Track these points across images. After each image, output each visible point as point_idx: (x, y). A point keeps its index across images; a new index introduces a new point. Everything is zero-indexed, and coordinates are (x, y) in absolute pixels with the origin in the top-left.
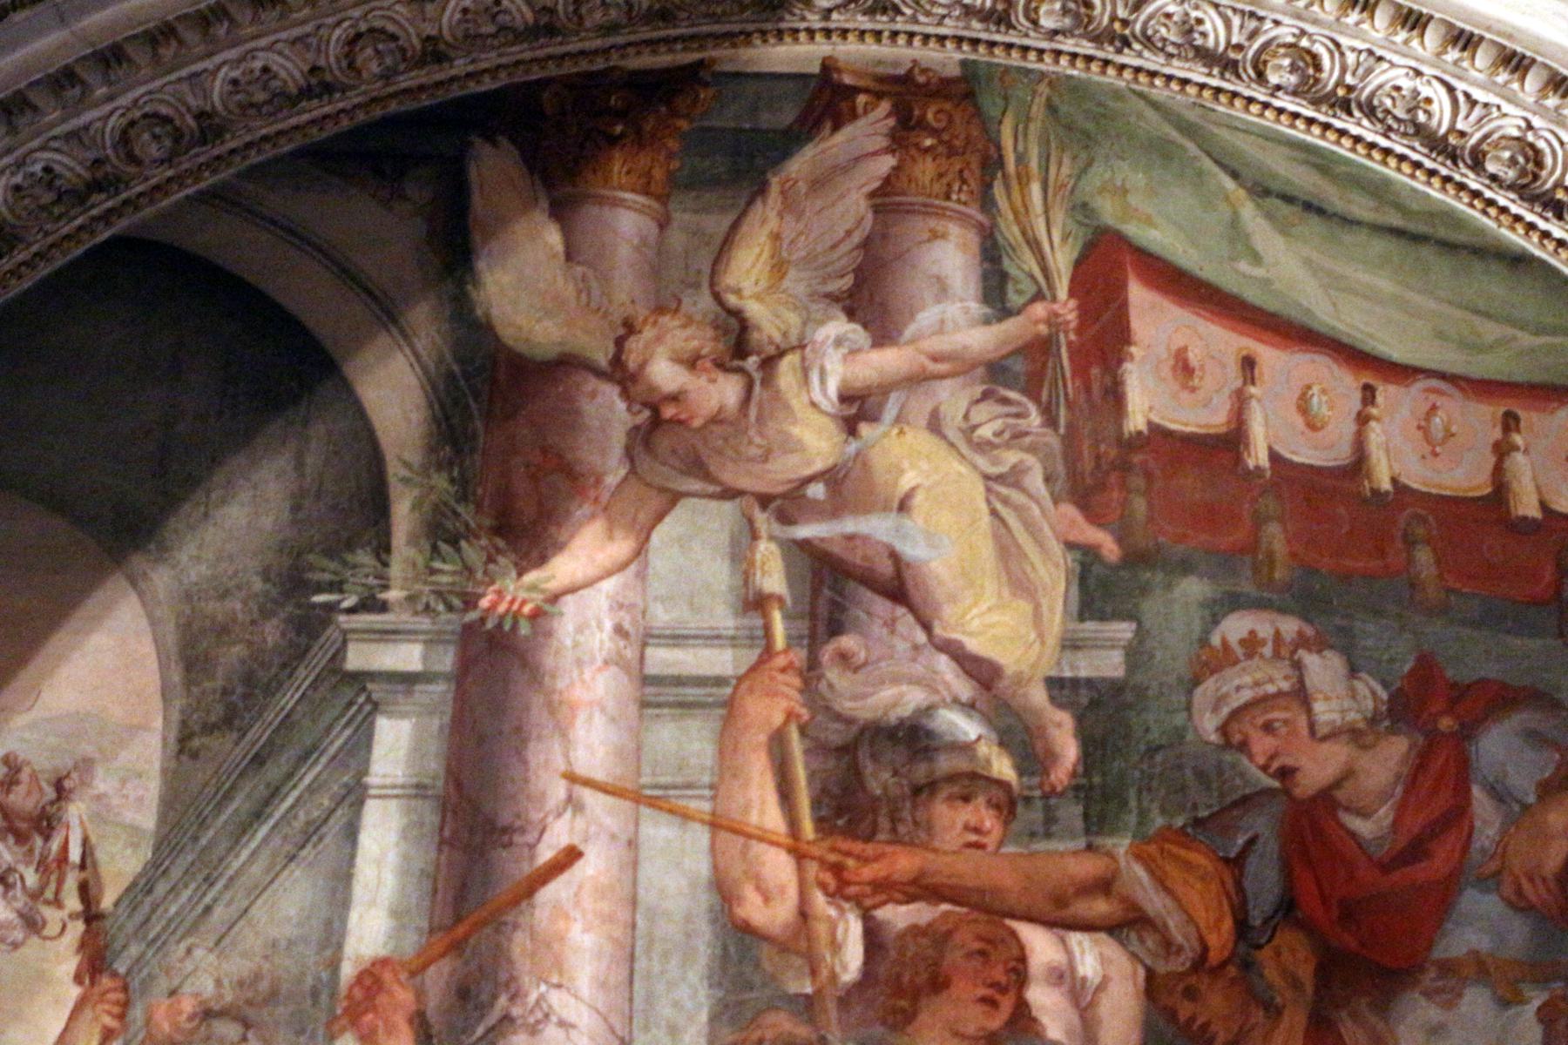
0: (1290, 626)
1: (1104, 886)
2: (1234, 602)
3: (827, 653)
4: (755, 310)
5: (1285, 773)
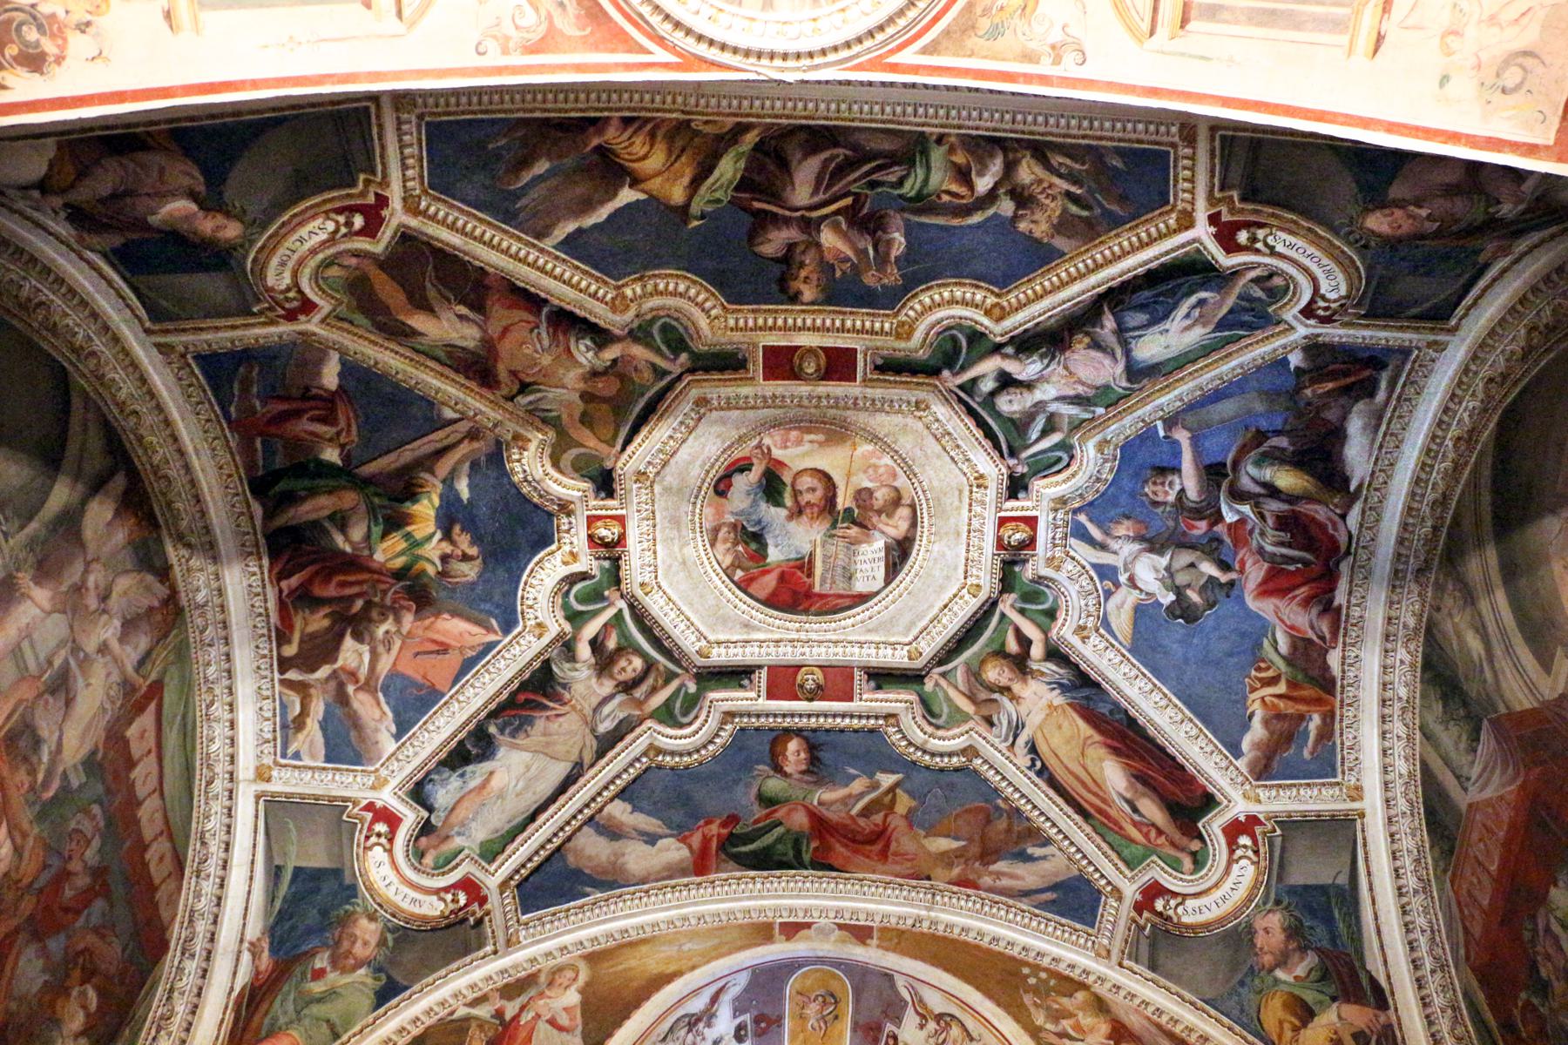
0: (102, 824)
1: (24, 835)
2: (100, 802)
3: (46, 696)
4: (114, 595)
5: (70, 858)
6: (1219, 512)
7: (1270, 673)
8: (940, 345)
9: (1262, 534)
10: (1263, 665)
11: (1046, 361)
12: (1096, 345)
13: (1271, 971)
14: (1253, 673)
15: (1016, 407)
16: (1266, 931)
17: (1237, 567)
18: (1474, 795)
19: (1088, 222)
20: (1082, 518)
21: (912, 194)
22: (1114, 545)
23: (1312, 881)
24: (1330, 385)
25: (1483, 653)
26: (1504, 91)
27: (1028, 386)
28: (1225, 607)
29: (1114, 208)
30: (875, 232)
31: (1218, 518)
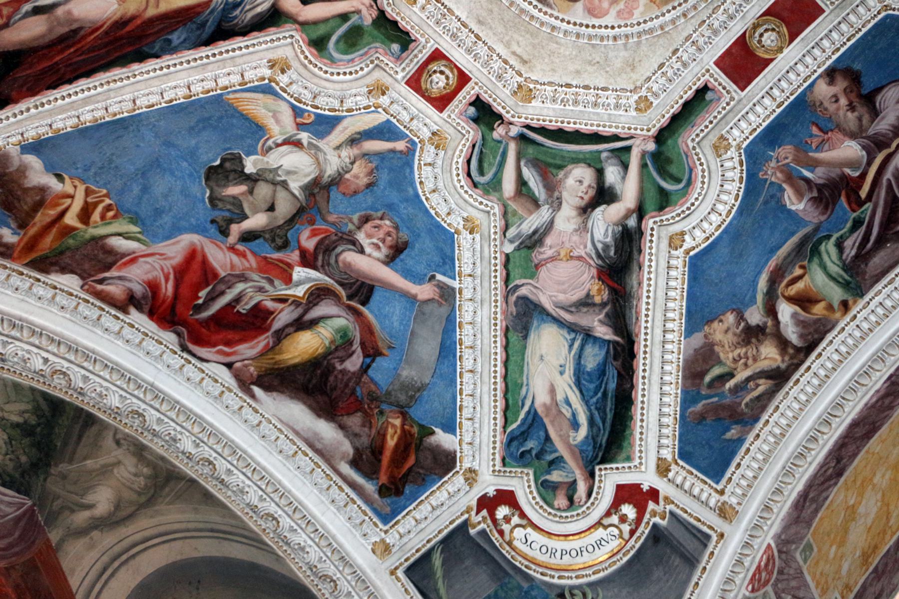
6: (314, 268)
7: (96, 216)
8: (681, 162)
9: (261, 290)
11: (600, 246)
12: (585, 303)
14: (108, 201)
15: (570, 182)
17: (240, 247)
19: (701, 375)
20: (400, 145)
21: (822, 248)
22: (347, 153)
24: (391, 442)
27: (586, 210)
28: (204, 212)
29: (699, 407)
30: (819, 191)
31: (308, 261)
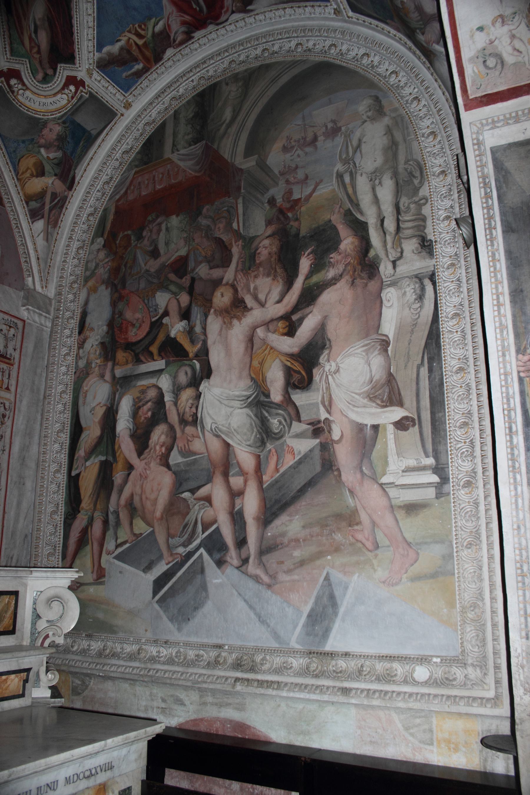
7: (142, 33)
10: (143, 26)
13: (40, 146)
14: (137, 26)
16: (51, 130)
18: (175, 157)
23: (82, 124)
25: (227, 121)
26: (485, 62)
